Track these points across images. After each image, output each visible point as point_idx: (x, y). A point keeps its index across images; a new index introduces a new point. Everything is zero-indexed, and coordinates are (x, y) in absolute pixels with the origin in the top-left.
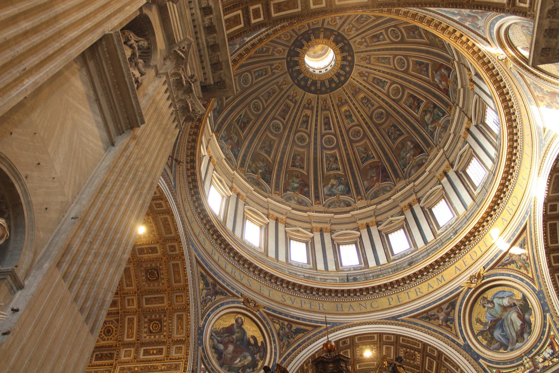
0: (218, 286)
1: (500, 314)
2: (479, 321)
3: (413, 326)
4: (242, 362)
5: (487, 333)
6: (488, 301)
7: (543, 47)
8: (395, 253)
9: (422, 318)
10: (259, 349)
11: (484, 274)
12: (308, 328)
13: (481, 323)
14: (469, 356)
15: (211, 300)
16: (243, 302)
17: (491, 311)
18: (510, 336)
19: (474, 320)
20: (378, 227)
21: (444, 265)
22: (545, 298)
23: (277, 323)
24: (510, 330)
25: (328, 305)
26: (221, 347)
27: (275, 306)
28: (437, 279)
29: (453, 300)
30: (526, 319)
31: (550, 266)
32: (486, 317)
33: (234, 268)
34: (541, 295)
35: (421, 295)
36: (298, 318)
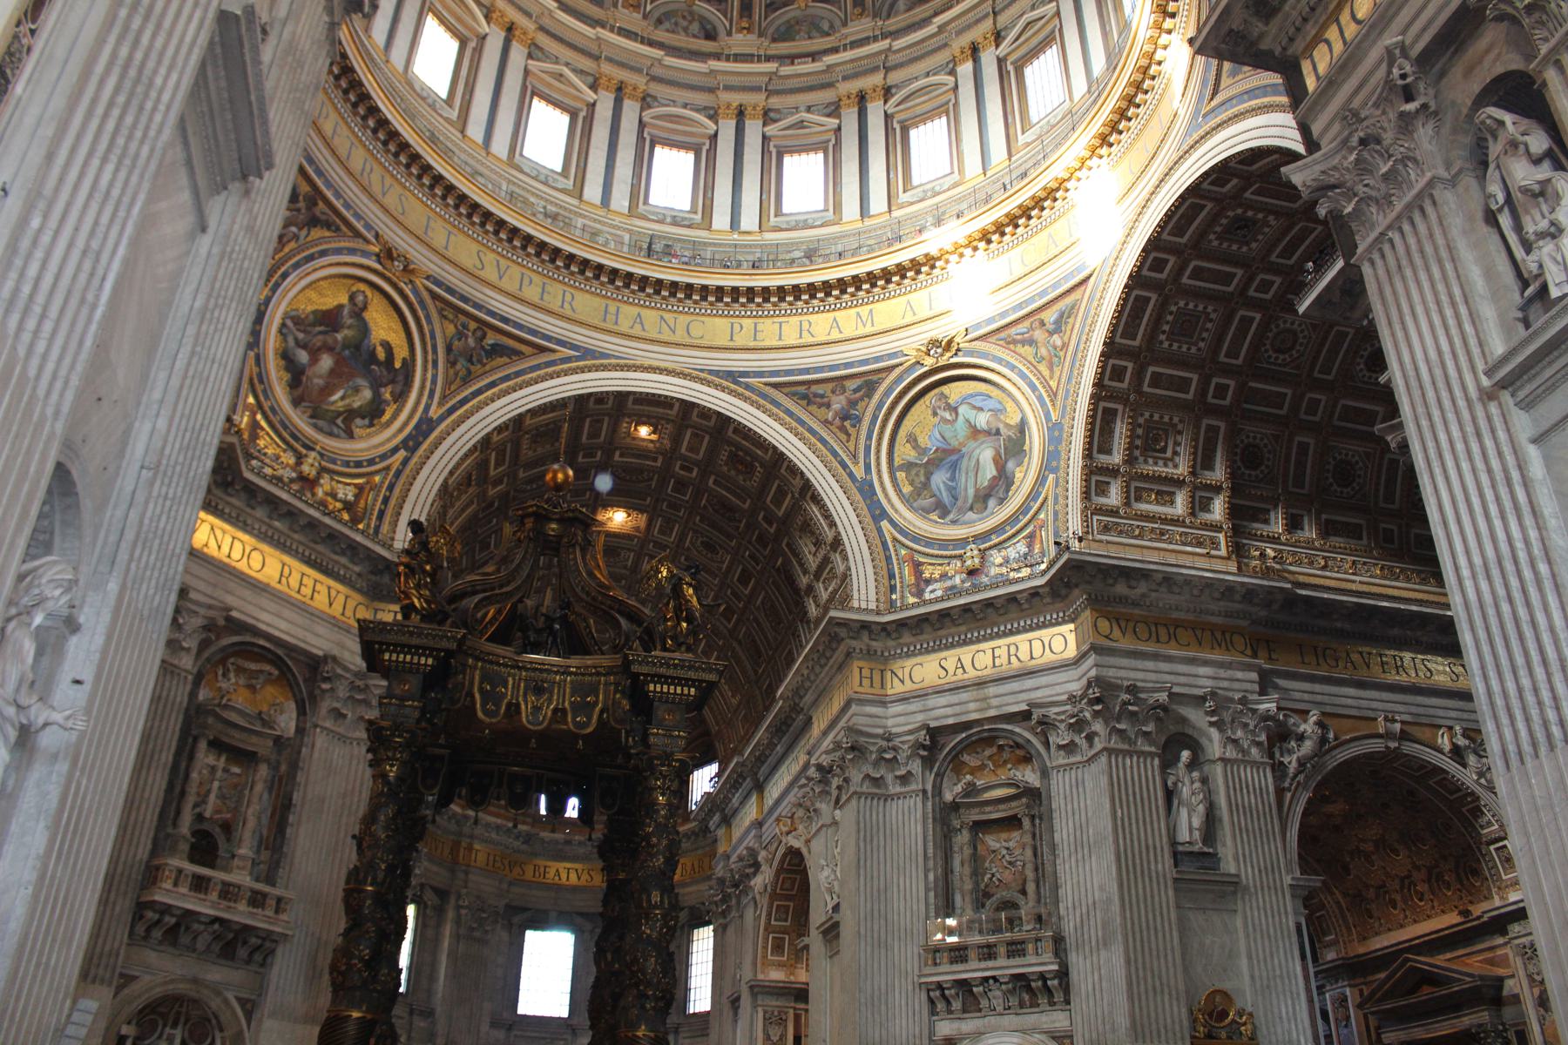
0: (321, 204)
2: (912, 439)
3: (769, 406)
4: (347, 401)
6: (948, 405)
7: (1234, 27)
8: (786, 209)
9: (794, 394)
10: (395, 376)
12: (523, 348)
13: (916, 446)
15: (296, 237)
16: (378, 255)
17: (946, 428)
19: (902, 433)
20: (764, 125)
21: (884, 288)
22: (1060, 443)
23: (452, 321)
25: (587, 303)
26: (303, 356)
27: (454, 278)
28: (858, 314)
29: (875, 378)
31: (1098, 384)
33: (370, 159)
34: (1056, 433)
35: (811, 340)
36: (506, 320)
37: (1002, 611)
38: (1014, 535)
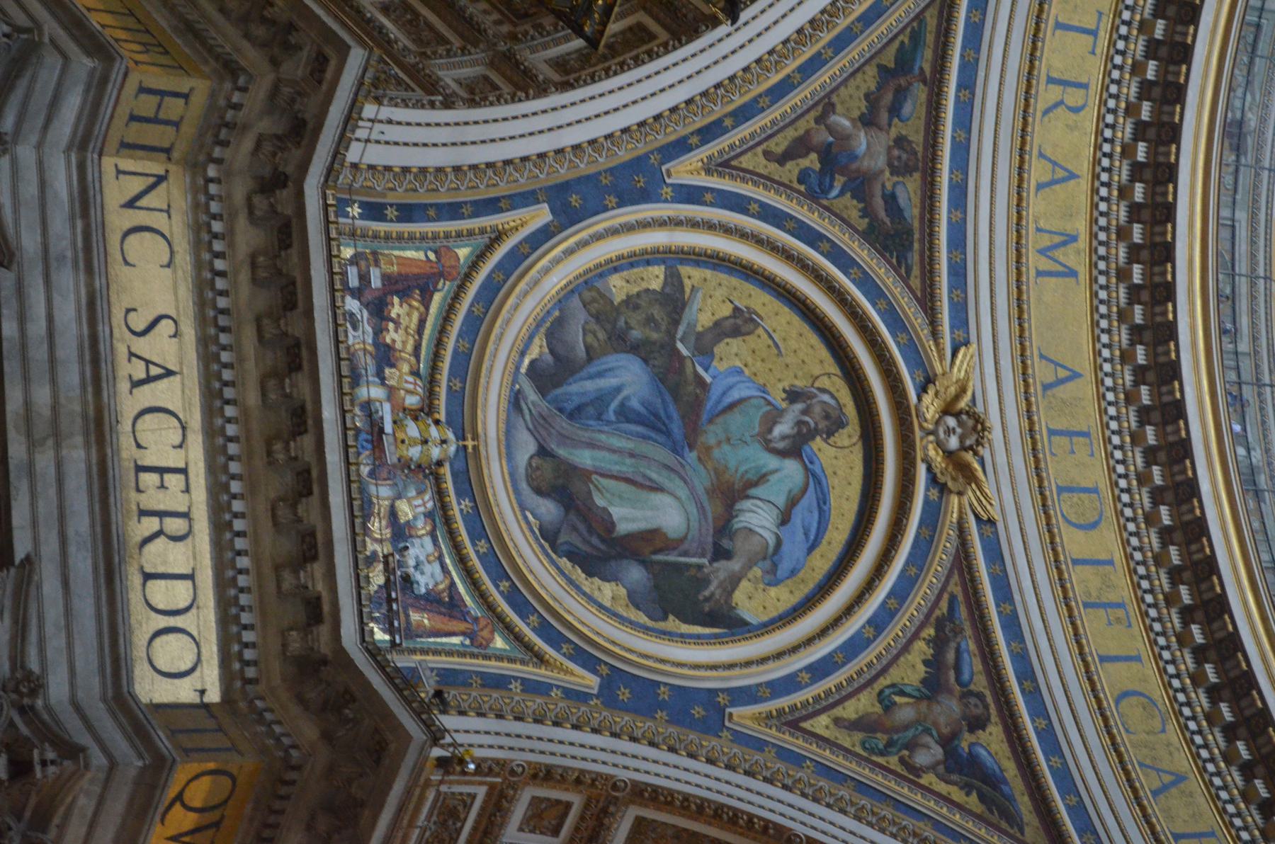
1: (716, 453)
5: (657, 327)
6: (812, 434)
9: (916, 37)
11: (955, 500)
14: (592, 170)
17: (754, 417)
18: (585, 435)
19: (760, 301)
24: (613, 451)
28: (1074, 239)
29: (914, 258)
30: (625, 562)
32: (741, 372)
34: (698, 712)
35: (1040, 104)
37: (284, 512)
38: (462, 560)
